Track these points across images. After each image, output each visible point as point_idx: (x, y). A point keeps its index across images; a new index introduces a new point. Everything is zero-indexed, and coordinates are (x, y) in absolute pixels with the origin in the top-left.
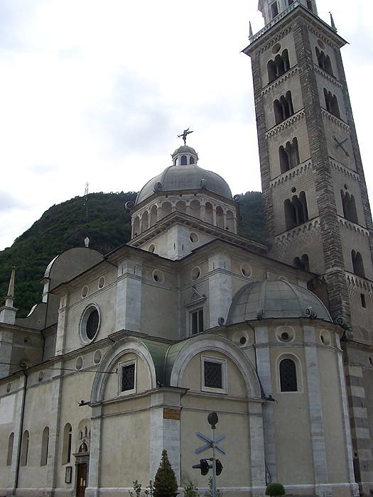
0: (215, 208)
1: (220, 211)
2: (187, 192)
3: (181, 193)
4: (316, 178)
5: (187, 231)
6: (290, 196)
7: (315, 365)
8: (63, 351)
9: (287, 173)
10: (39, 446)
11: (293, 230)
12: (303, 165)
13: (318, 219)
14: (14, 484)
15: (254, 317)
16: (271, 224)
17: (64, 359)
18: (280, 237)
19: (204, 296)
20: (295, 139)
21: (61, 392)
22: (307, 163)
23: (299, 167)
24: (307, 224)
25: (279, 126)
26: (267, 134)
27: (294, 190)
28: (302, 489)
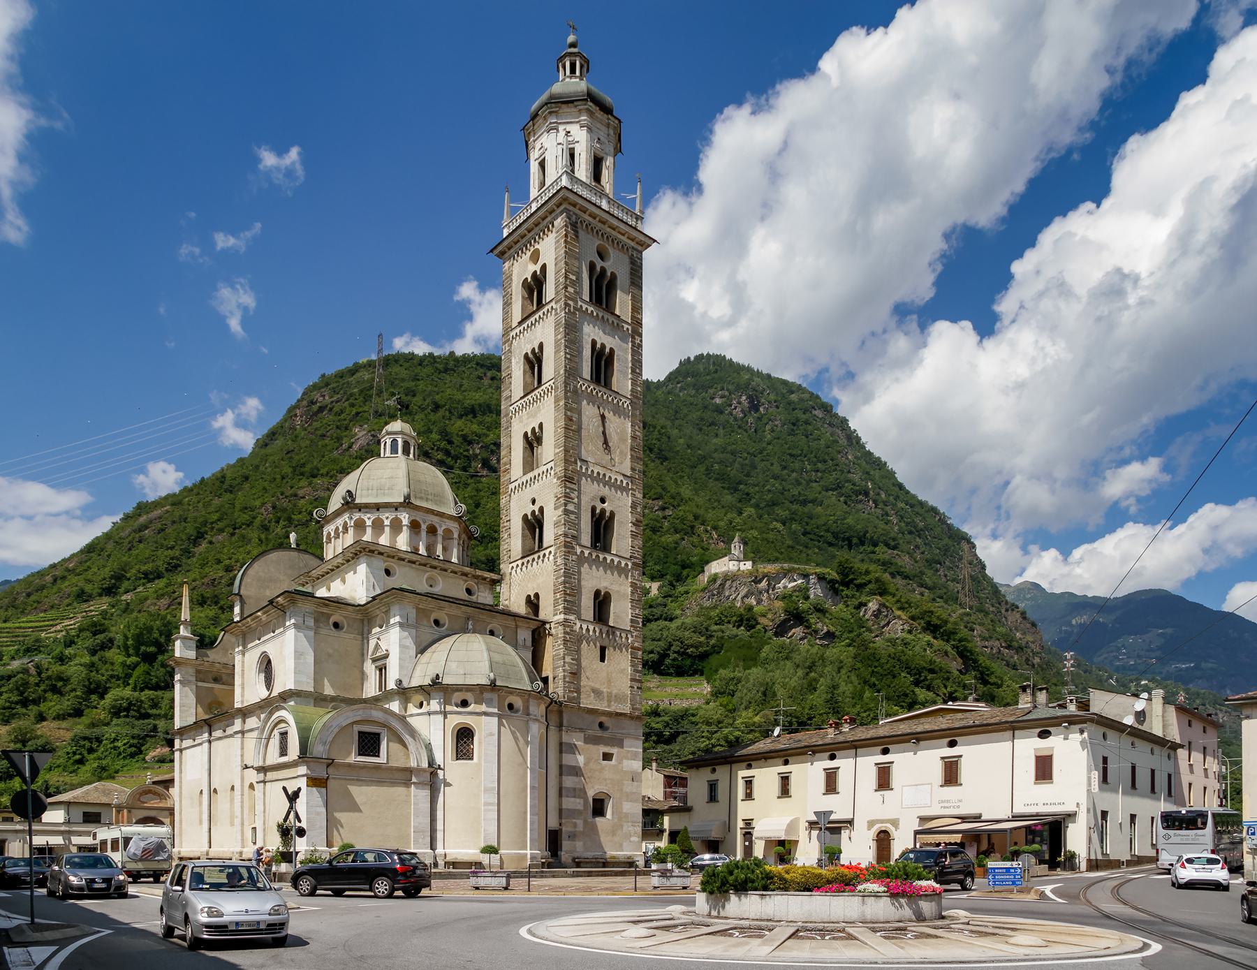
0: (424, 527)
1: (432, 530)
2: (387, 506)
3: (378, 507)
4: (555, 491)
5: (381, 564)
6: (529, 509)
7: (493, 735)
8: (242, 702)
9: (531, 475)
10: (228, 805)
11: (532, 557)
12: (544, 468)
13: (552, 549)
14: (207, 845)
15: (427, 681)
16: (506, 546)
17: (245, 713)
18: (514, 565)
19: (387, 651)
20: (541, 426)
21: (242, 748)
22: (549, 466)
23: (540, 470)
24: (541, 554)
25: (525, 399)
26: (511, 408)
27: (534, 502)
28: (467, 854)
